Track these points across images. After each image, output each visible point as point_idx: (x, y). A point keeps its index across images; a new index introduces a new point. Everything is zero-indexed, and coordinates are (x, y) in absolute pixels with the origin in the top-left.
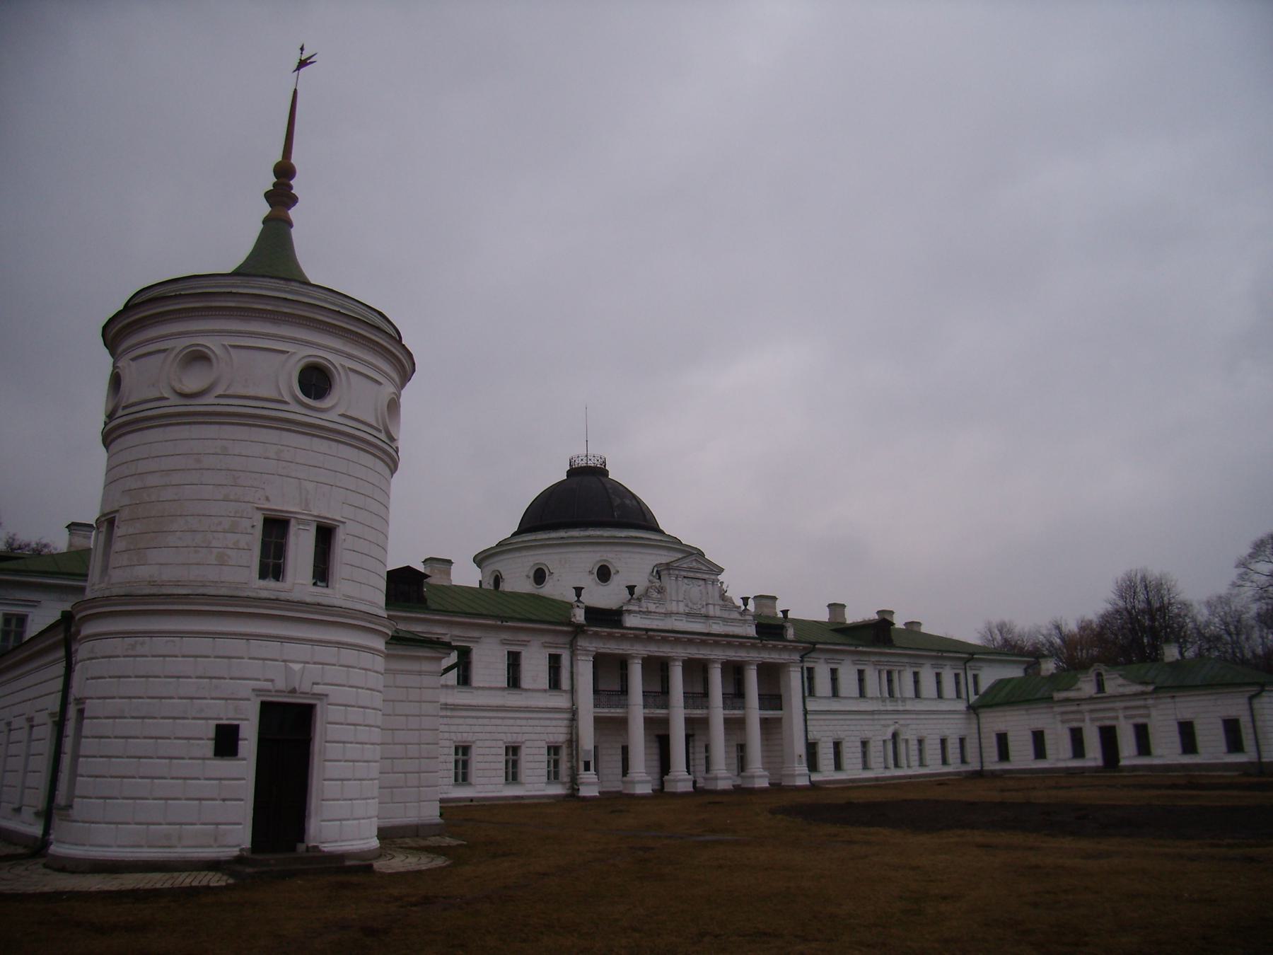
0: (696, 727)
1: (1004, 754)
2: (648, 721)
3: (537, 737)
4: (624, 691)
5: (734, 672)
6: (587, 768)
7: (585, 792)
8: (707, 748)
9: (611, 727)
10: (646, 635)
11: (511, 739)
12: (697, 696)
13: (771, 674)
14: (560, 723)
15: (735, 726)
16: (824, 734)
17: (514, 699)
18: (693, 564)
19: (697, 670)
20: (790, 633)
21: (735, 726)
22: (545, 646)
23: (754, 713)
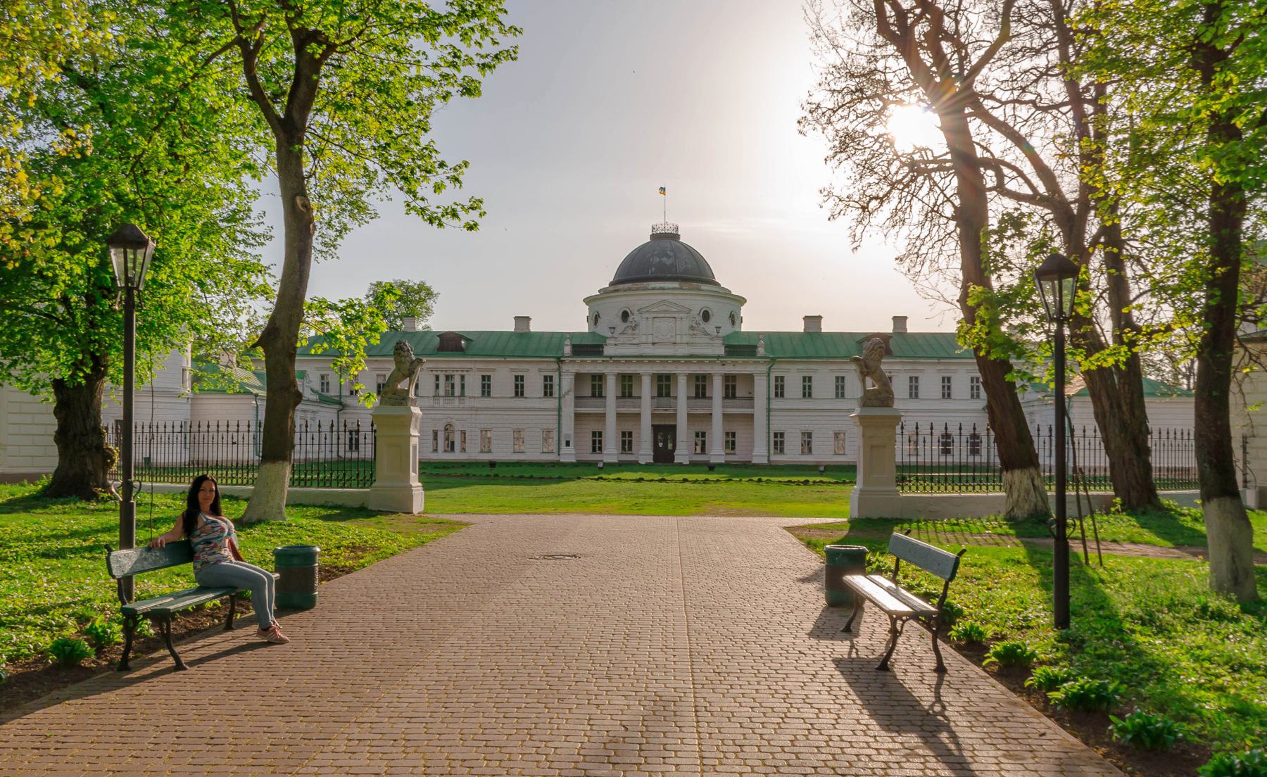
6: (568, 444)
7: (563, 459)
17: (520, 403)
20: (761, 351)
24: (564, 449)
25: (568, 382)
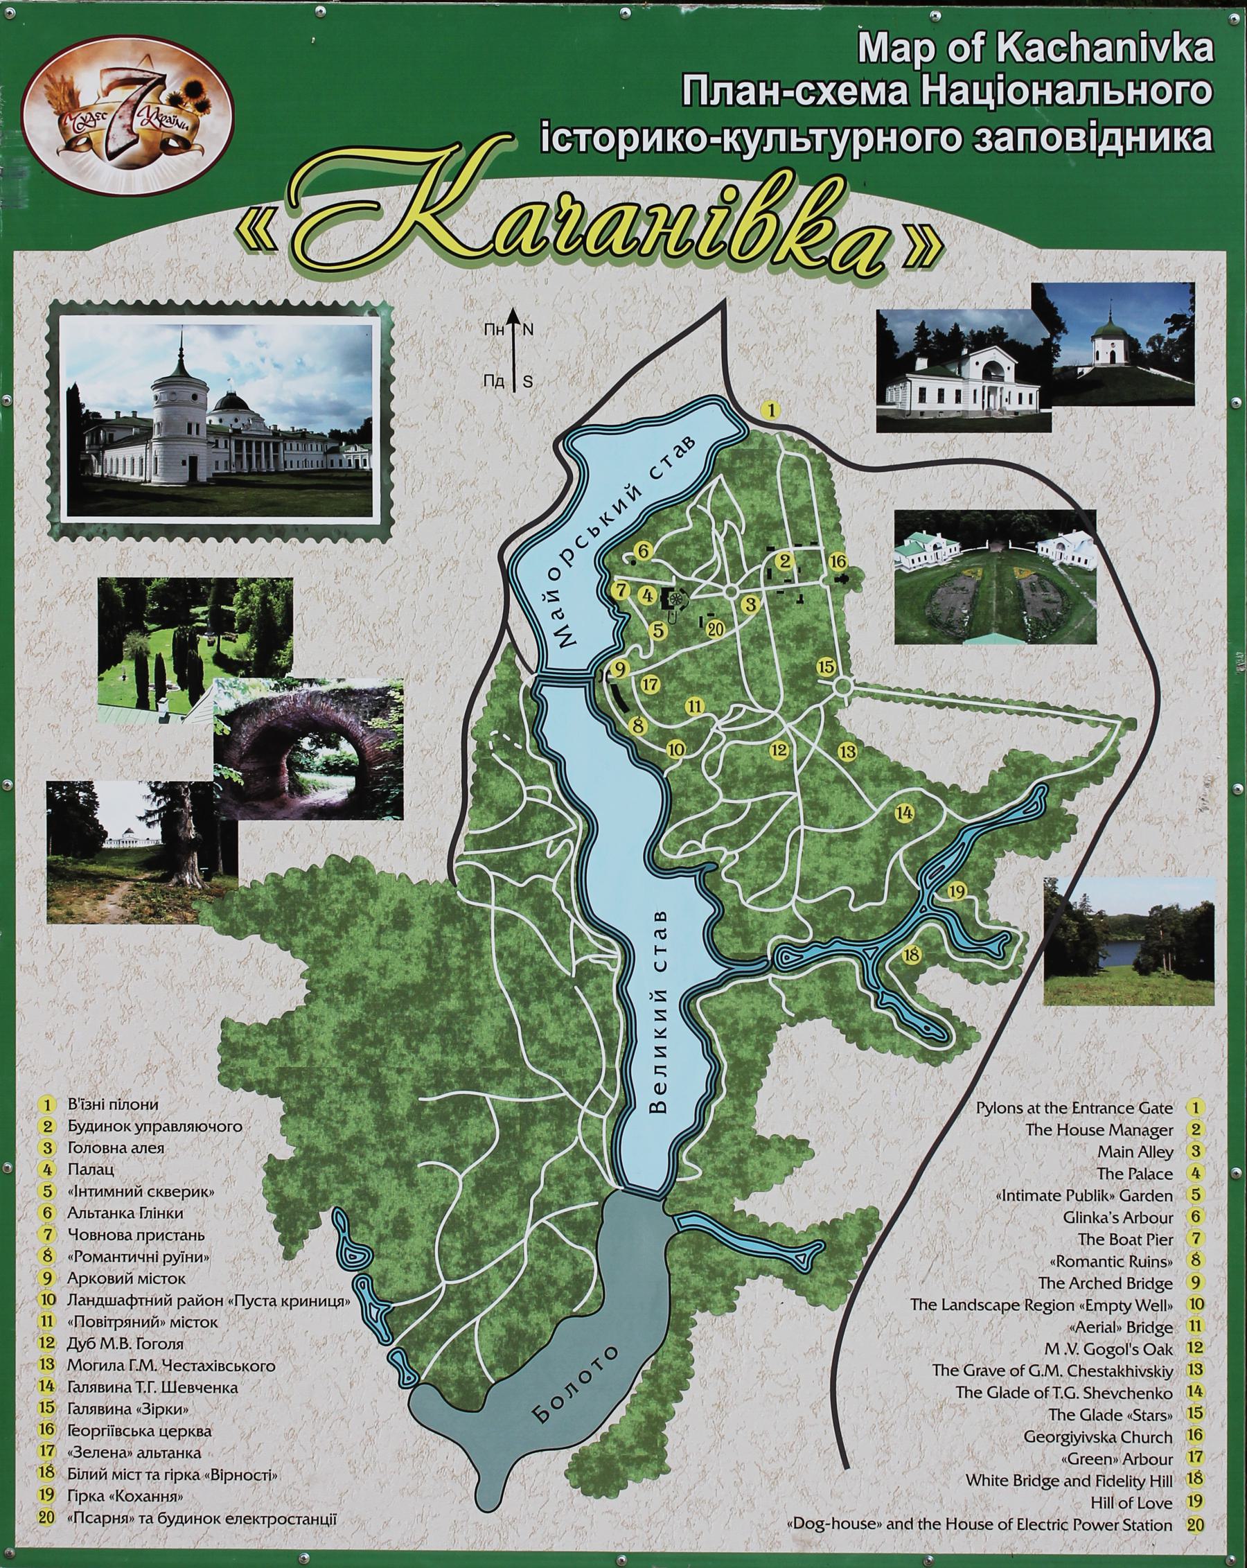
0: (258, 457)
9: (239, 457)
10: (247, 435)
12: (259, 450)
18: (258, 419)
19: (258, 444)
25: (233, 443)
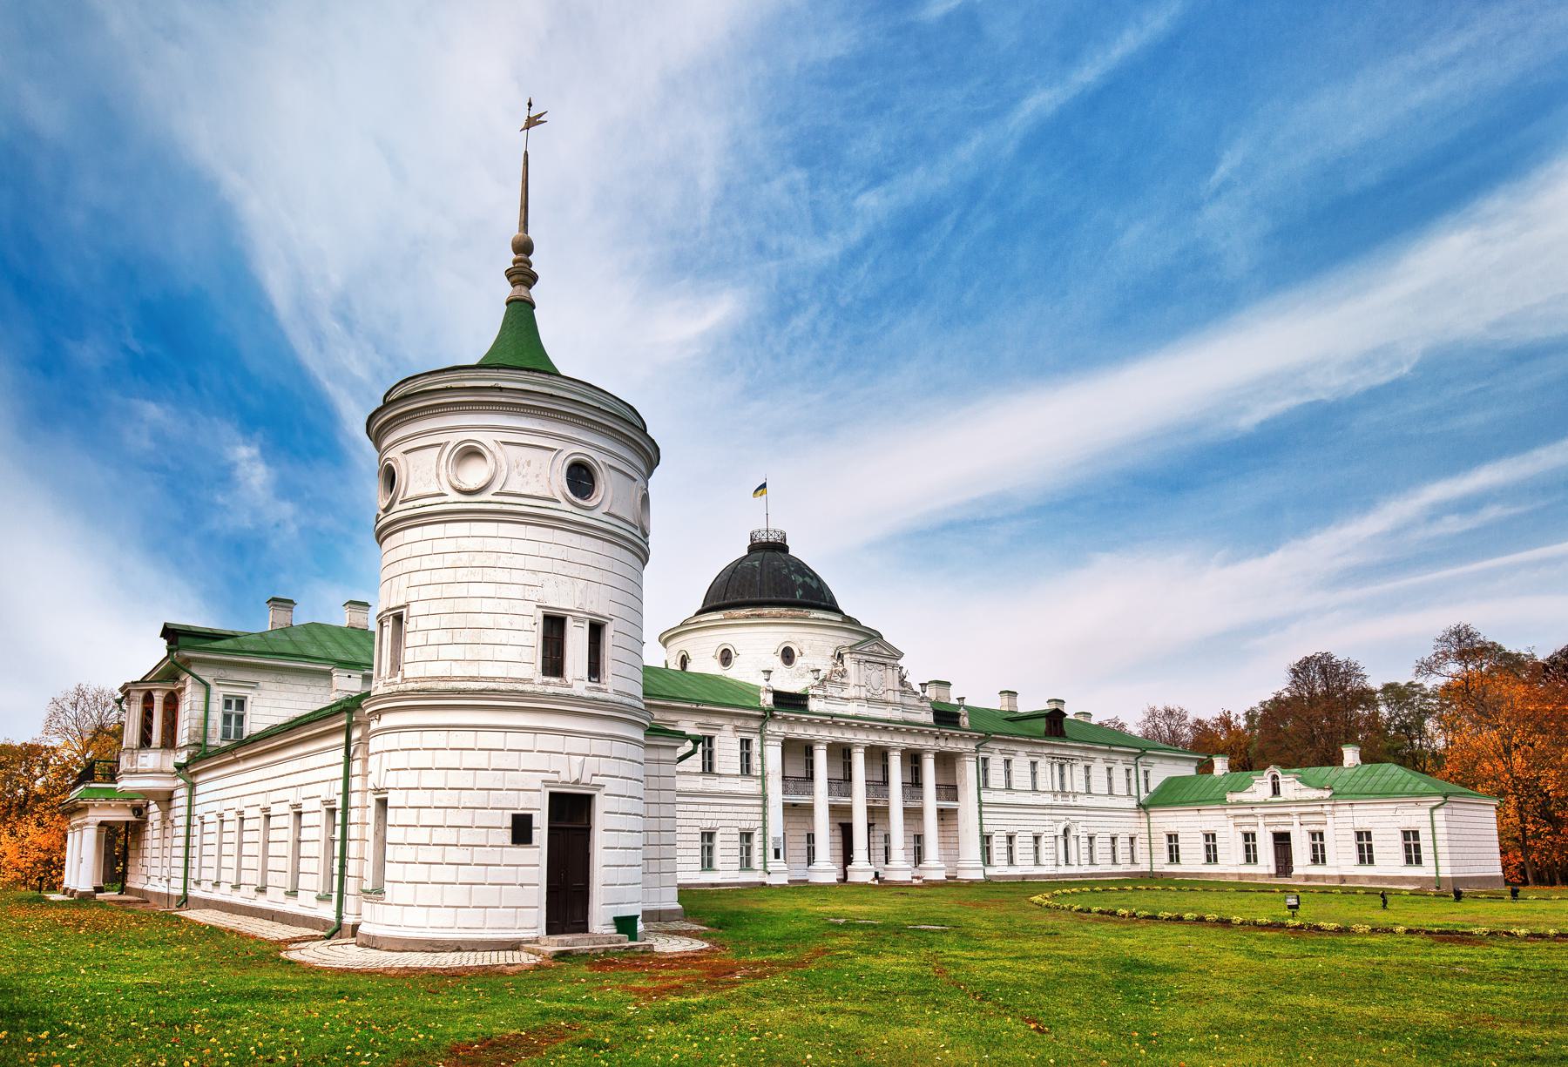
1: (1174, 857)
2: (833, 809)
3: (728, 823)
4: (810, 777)
5: (913, 760)
7: (769, 880)
8: (887, 837)
9: (798, 812)
10: (832, 721)
11: (707, 825)
12: (879, 784)
13: (946, 761)
14: (750, 809)
15: (913, 814)
16: (998, 825)
21: (913, 814)
22: (737, 729)
23: (930, 802)
24: (773, 864)
25: (774, 754)
